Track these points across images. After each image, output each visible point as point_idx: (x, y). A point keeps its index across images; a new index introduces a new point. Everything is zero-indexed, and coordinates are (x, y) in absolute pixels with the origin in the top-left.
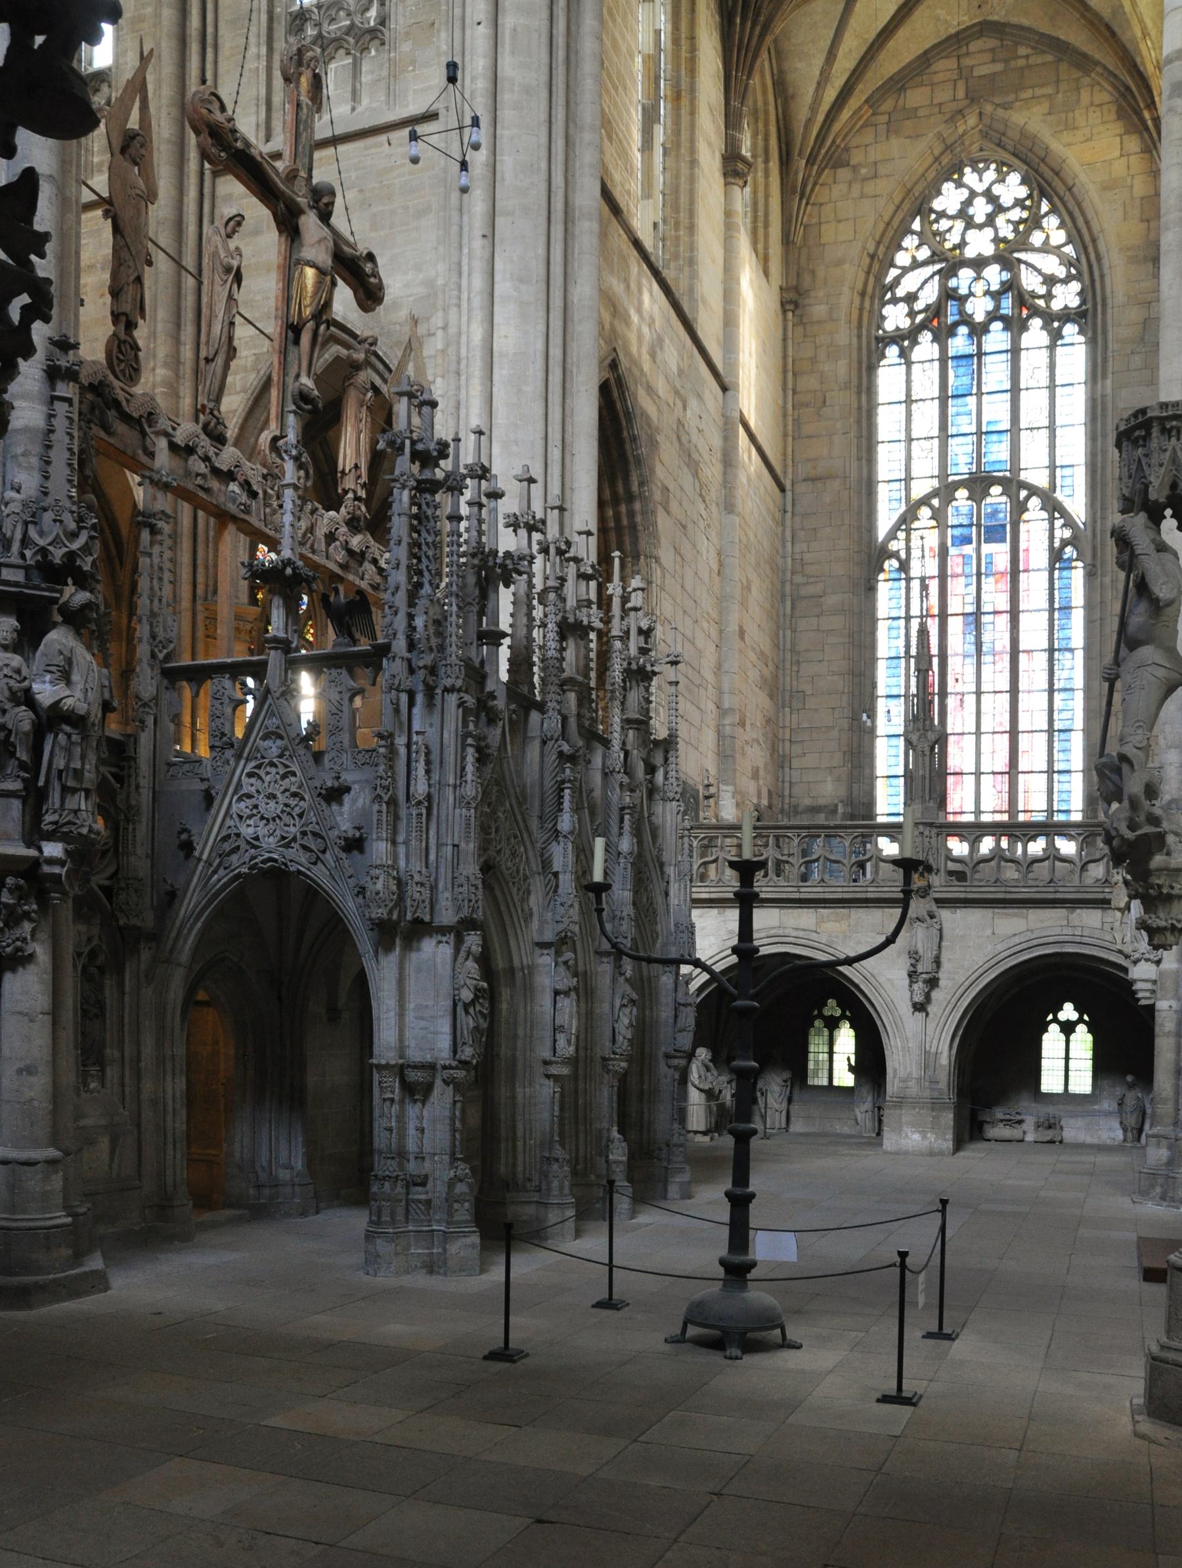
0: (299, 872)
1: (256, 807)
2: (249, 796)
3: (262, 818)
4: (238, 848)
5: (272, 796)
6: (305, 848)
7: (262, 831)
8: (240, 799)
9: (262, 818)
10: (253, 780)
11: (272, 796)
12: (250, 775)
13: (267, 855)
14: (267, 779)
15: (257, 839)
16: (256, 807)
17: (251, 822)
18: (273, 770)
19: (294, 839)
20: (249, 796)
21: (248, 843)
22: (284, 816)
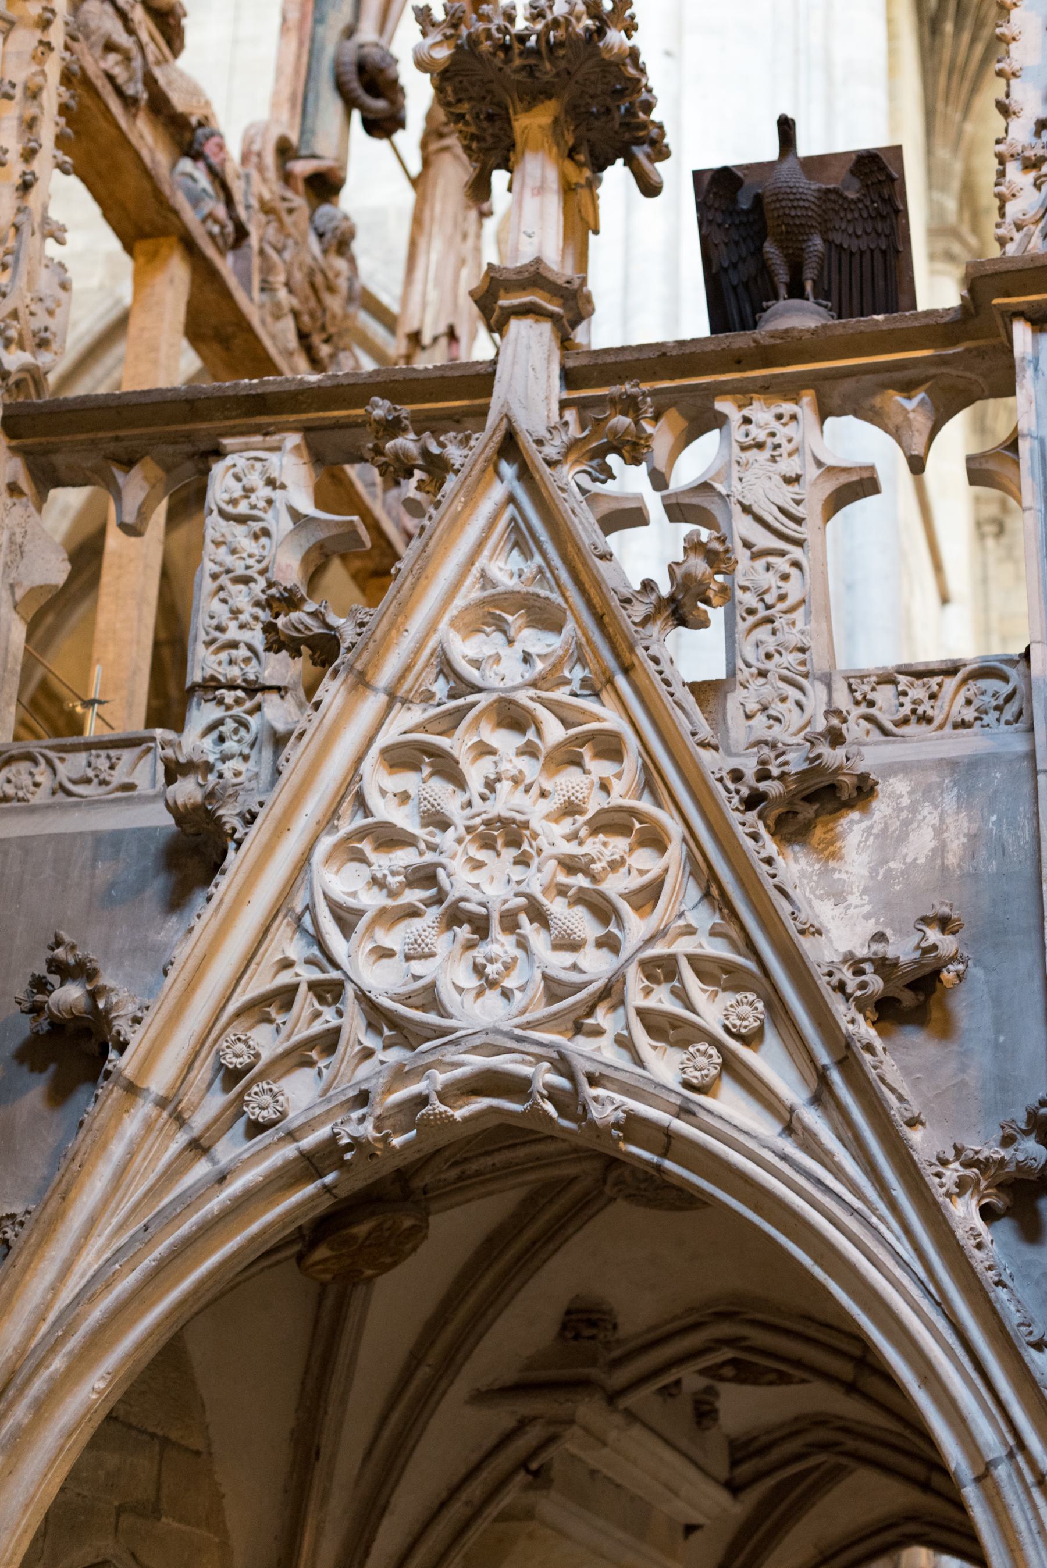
0: (633, 1126)
1: (425, 877)
2: (390, 838)
3: (454, 917)
4: (329, 1042)
5: (508, 834)
6: (660, 1027)
7: (450, 969)
8: (349, 852)
9: (454, 917)
10: (408, 781)
11: (508, 834)
12: (403, 757)
13: (478, 1062)
14: (475, 773)
15: (429, 997)
16: (425, 877)
17: (394, 938)
18: (505, 741)
19: (611, 993)
20: (390, 838)
21: (377, 1016)
22: (557, 907)
